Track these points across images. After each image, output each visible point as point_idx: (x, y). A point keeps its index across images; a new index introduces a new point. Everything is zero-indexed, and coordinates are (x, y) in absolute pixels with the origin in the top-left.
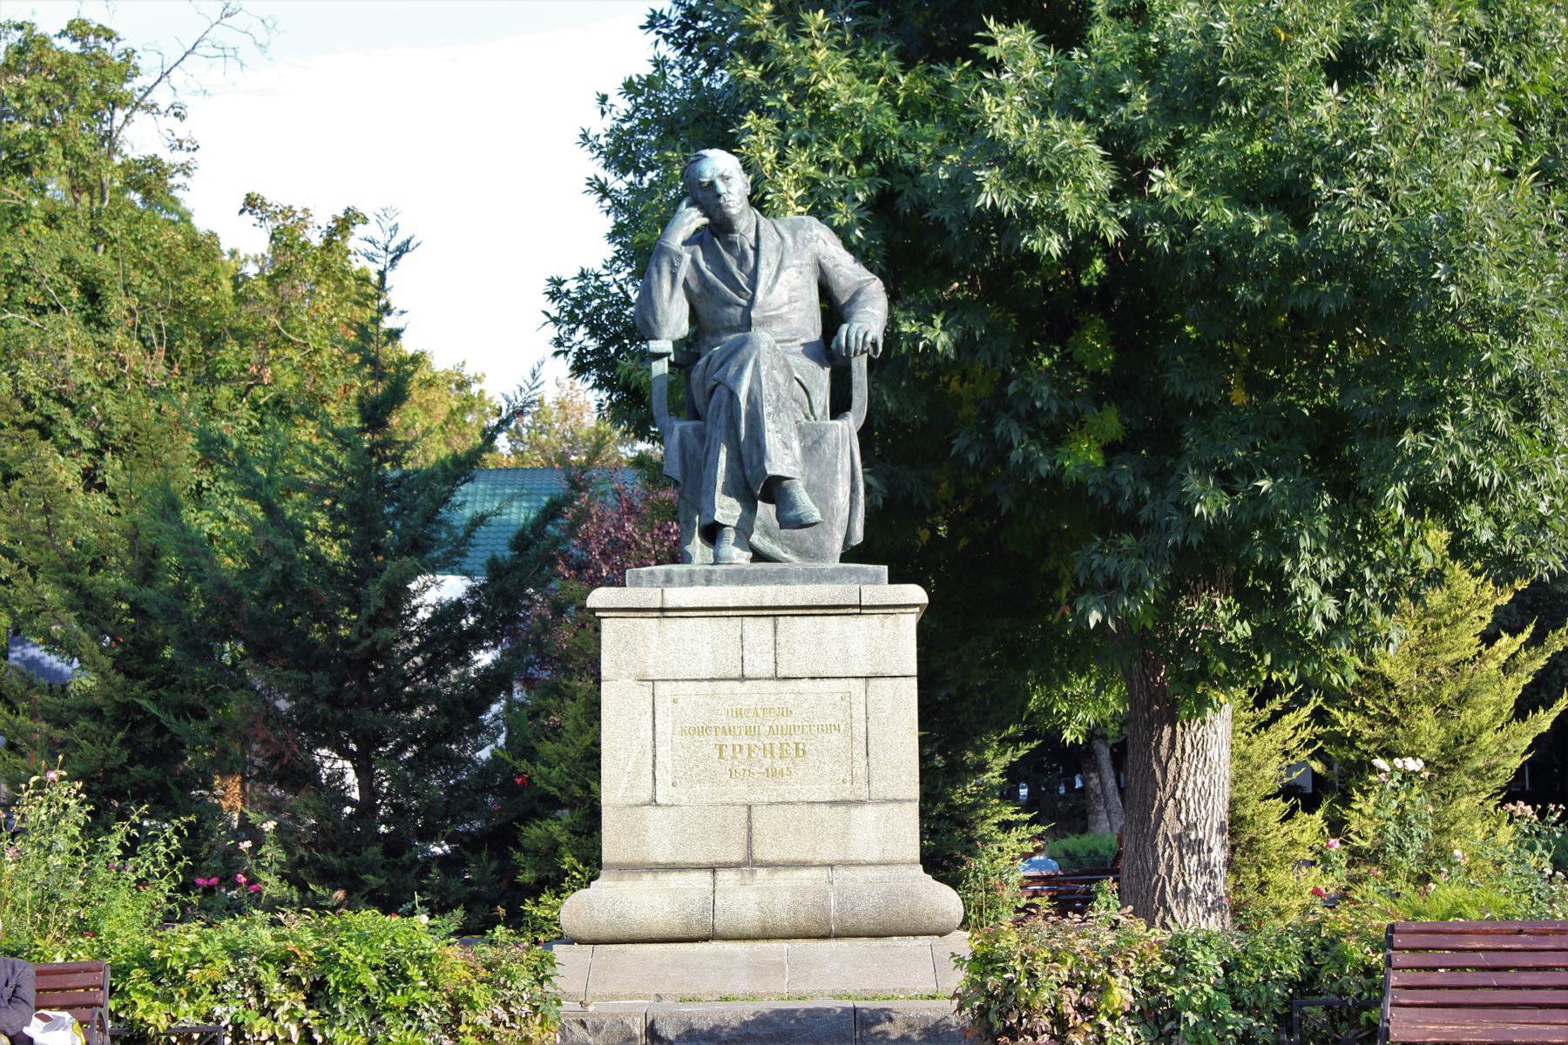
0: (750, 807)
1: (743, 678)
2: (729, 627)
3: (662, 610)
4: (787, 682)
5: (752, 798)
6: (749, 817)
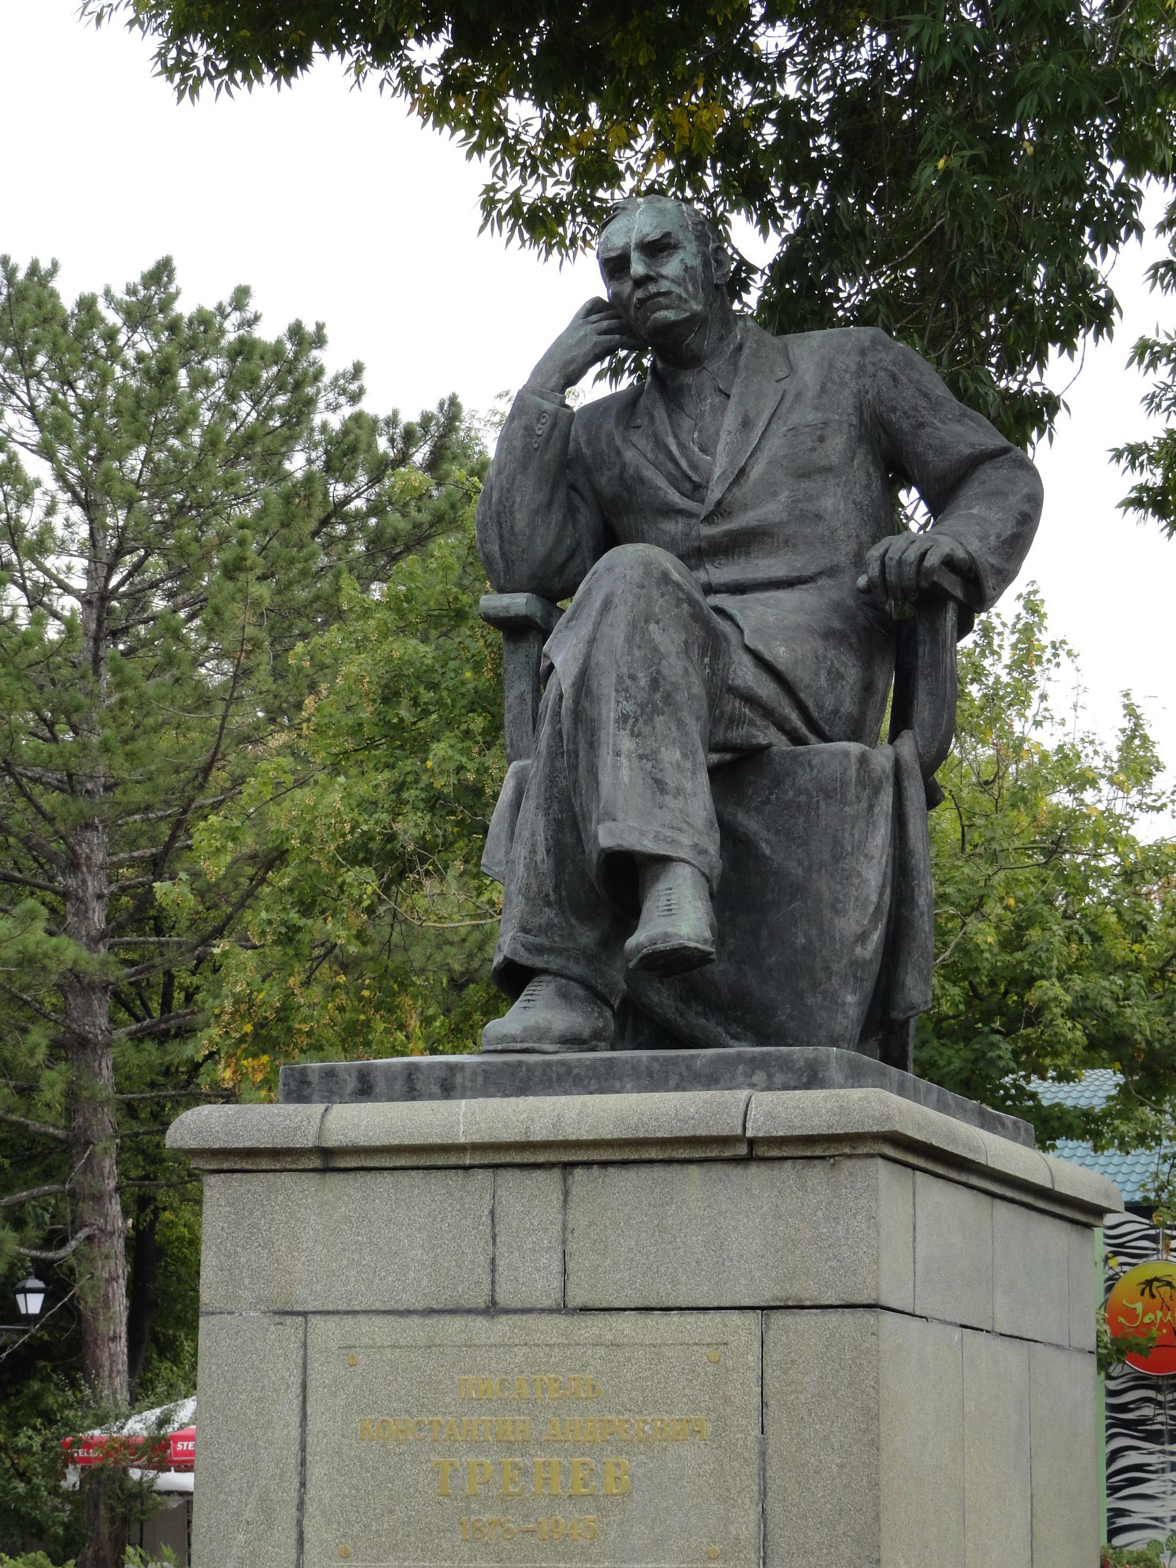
1: (492, 1309)
3: (327, 1153)
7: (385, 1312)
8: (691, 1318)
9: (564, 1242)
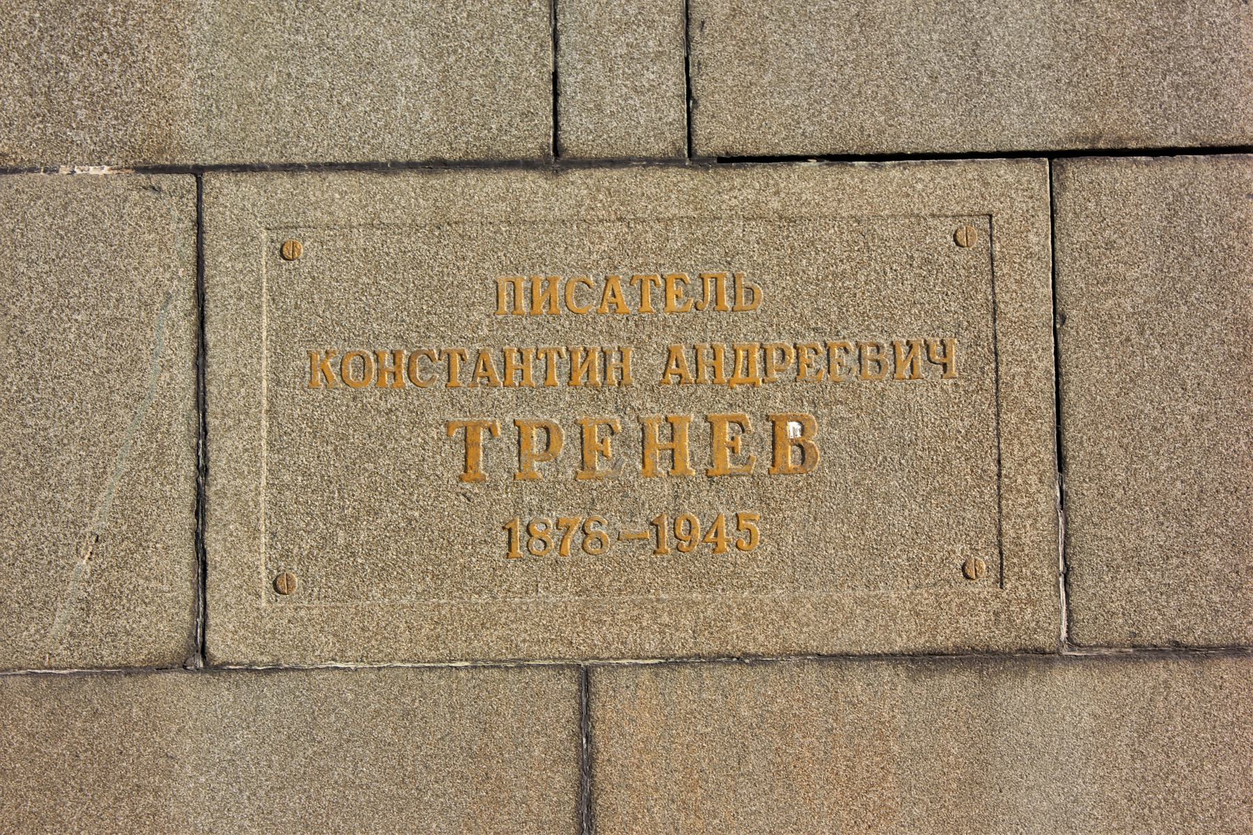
0: (585, 678)
4: (736, 177)
6: (585, 715)
7: (350, 167)
8: (923, 173)
9: (688, 41)
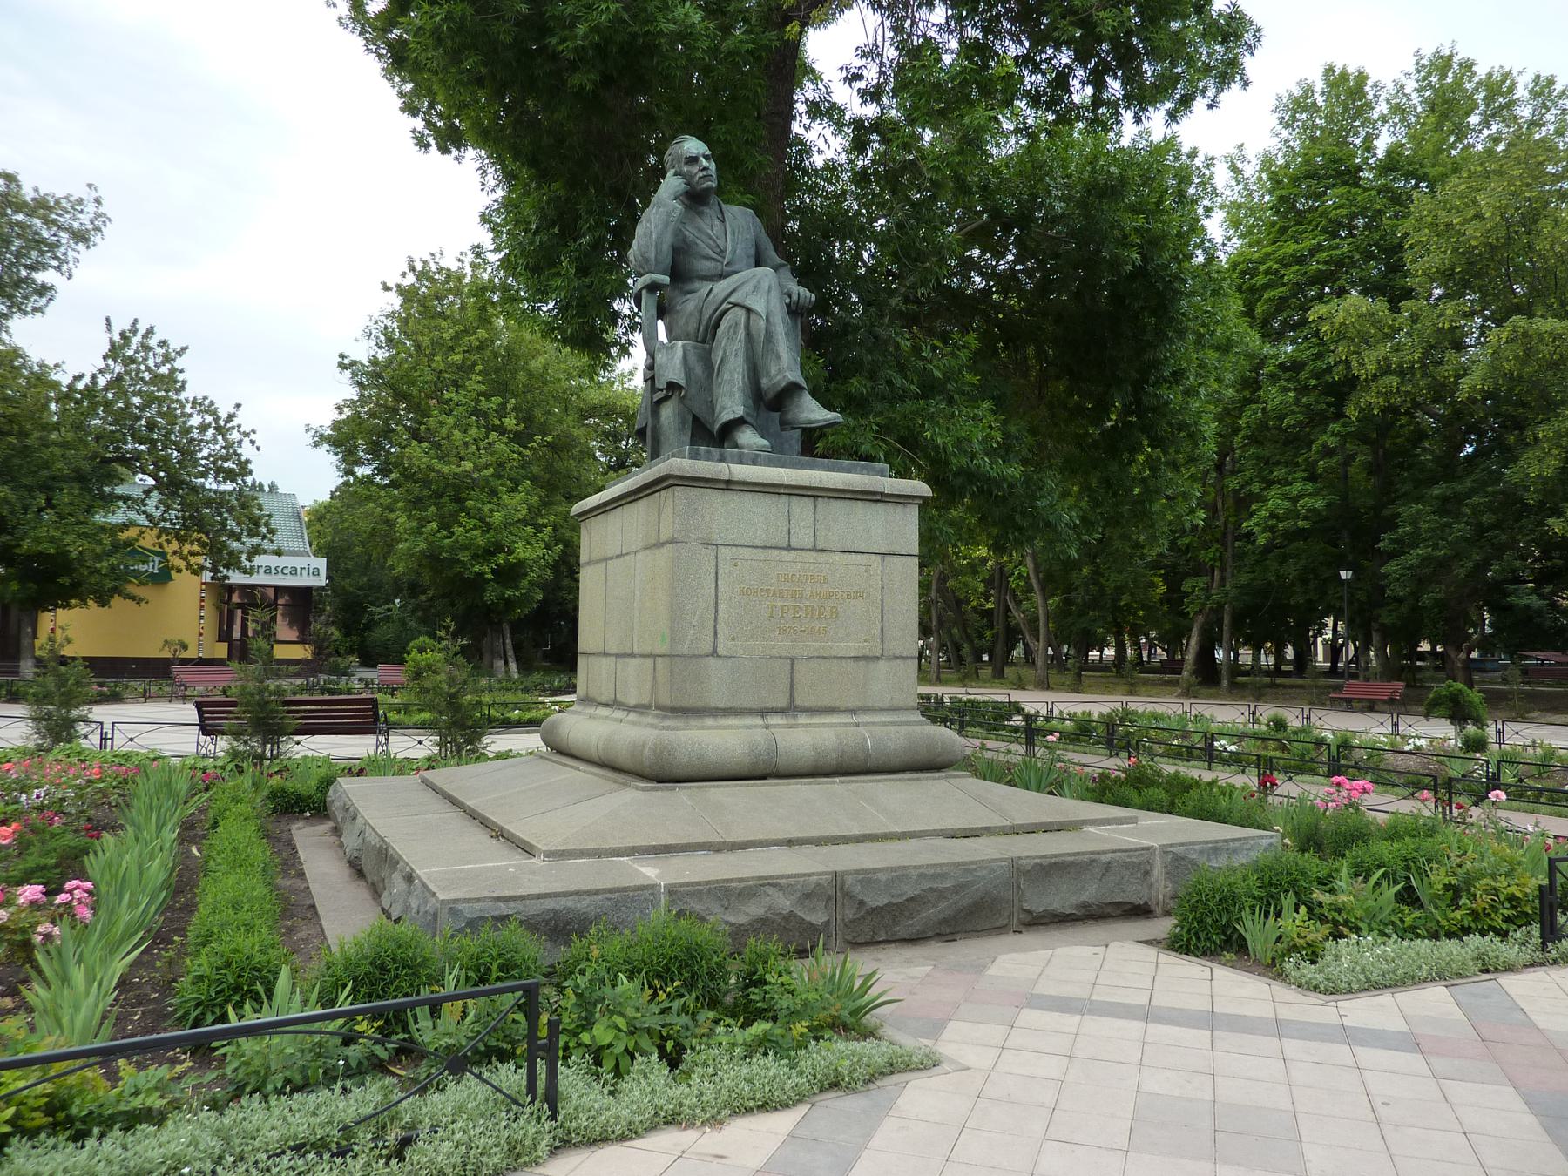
0: (792, 660)
1: (789, 548)
2: (640, 509)
3: (728, 482)
4: (824, 554)
5: (794, 652)
